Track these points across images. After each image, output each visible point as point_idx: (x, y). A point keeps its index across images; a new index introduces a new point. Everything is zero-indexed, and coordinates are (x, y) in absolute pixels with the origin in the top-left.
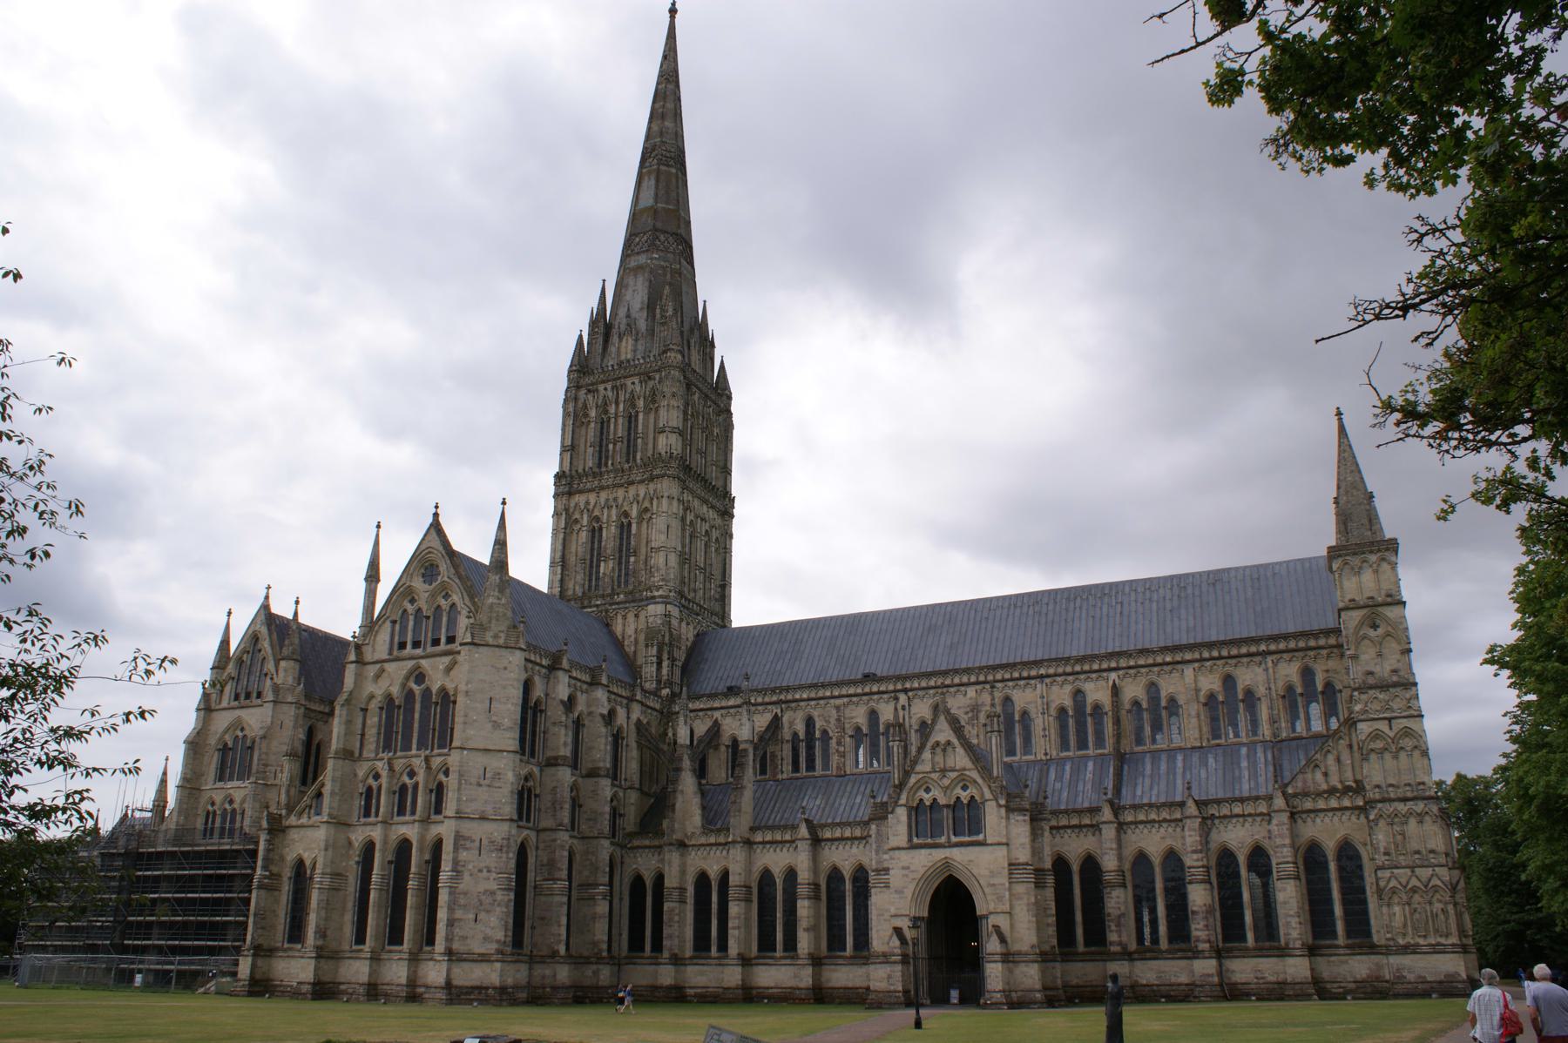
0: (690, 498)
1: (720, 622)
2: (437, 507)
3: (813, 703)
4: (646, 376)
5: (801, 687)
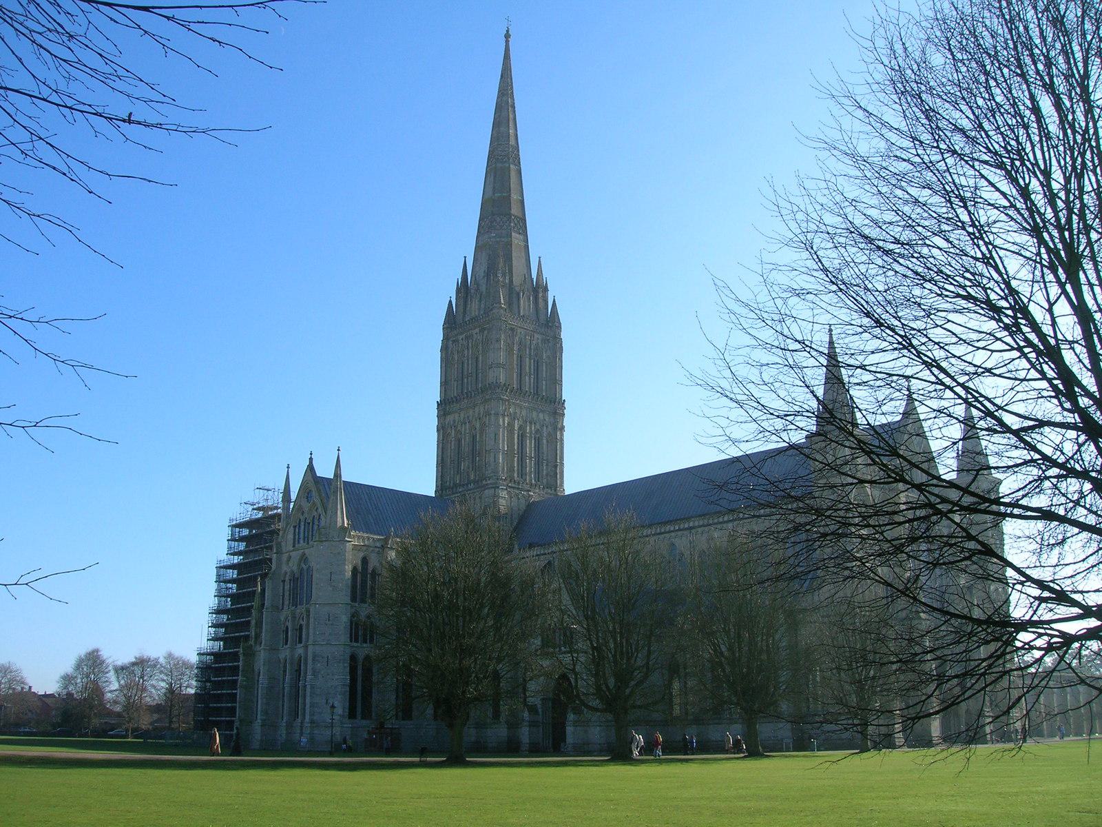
2: (311, 454)
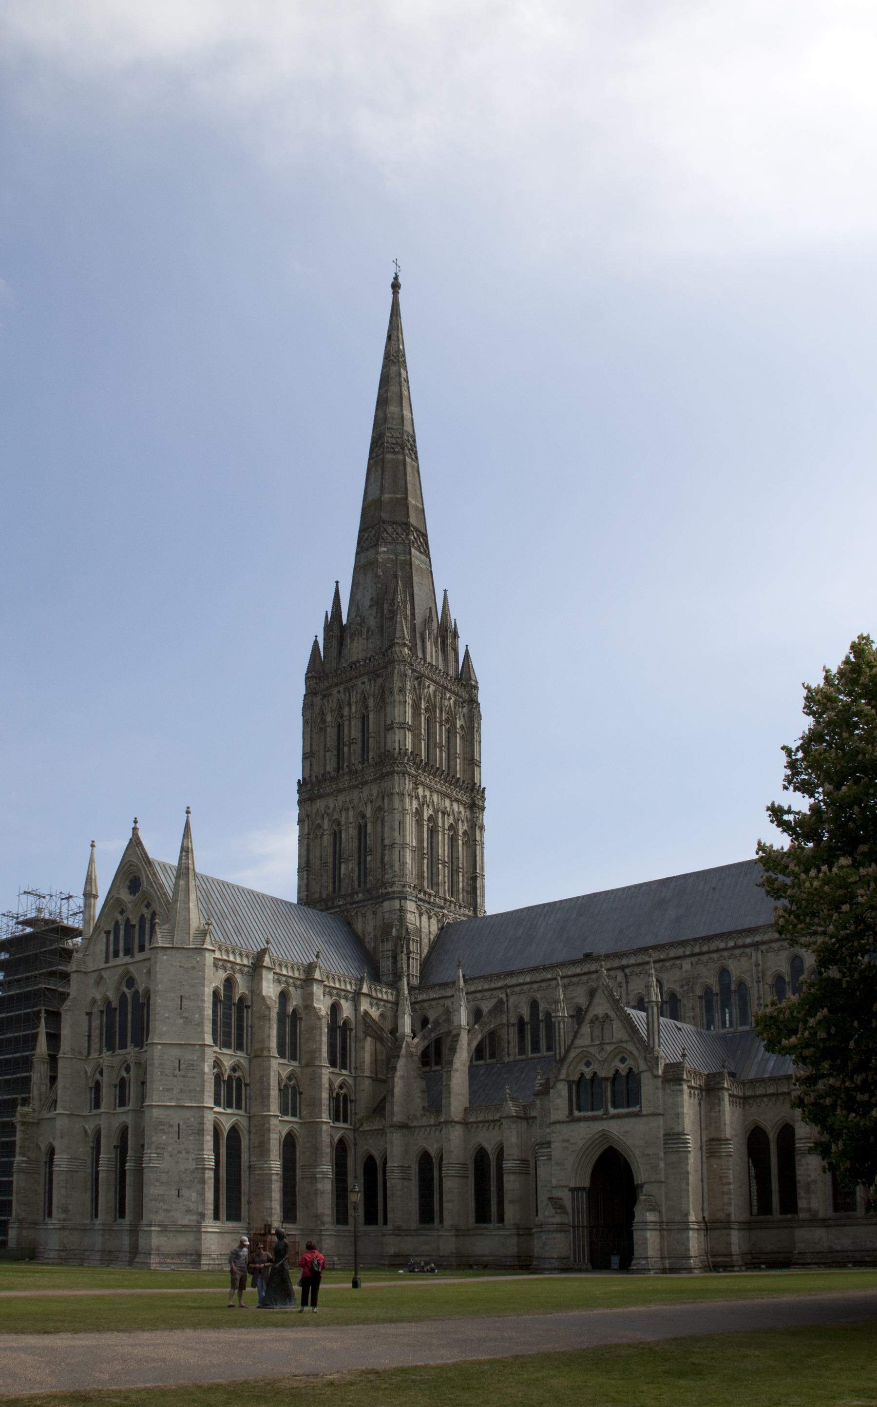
0: (427, 793)
1: (471, 913)
3: (535, 986)
4: (375, 675)
5: (522, 972)
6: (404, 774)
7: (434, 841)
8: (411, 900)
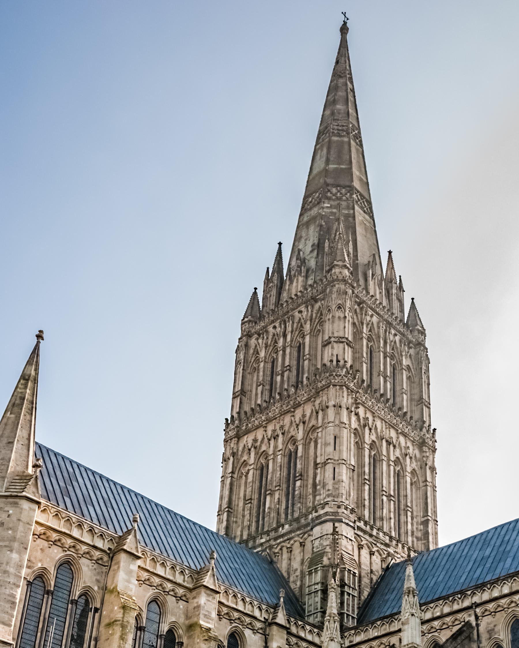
6: (341, 386)
7: (377, 471)
8: (347, 524)
